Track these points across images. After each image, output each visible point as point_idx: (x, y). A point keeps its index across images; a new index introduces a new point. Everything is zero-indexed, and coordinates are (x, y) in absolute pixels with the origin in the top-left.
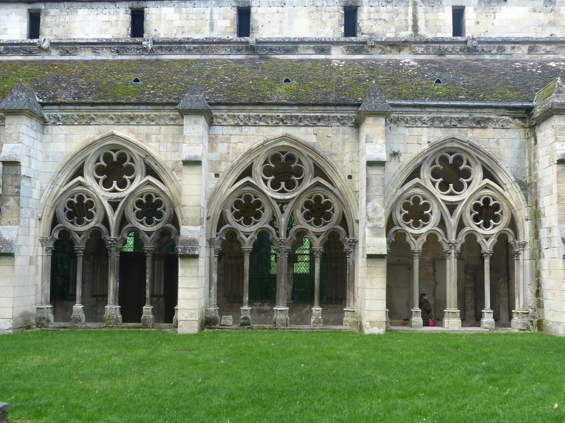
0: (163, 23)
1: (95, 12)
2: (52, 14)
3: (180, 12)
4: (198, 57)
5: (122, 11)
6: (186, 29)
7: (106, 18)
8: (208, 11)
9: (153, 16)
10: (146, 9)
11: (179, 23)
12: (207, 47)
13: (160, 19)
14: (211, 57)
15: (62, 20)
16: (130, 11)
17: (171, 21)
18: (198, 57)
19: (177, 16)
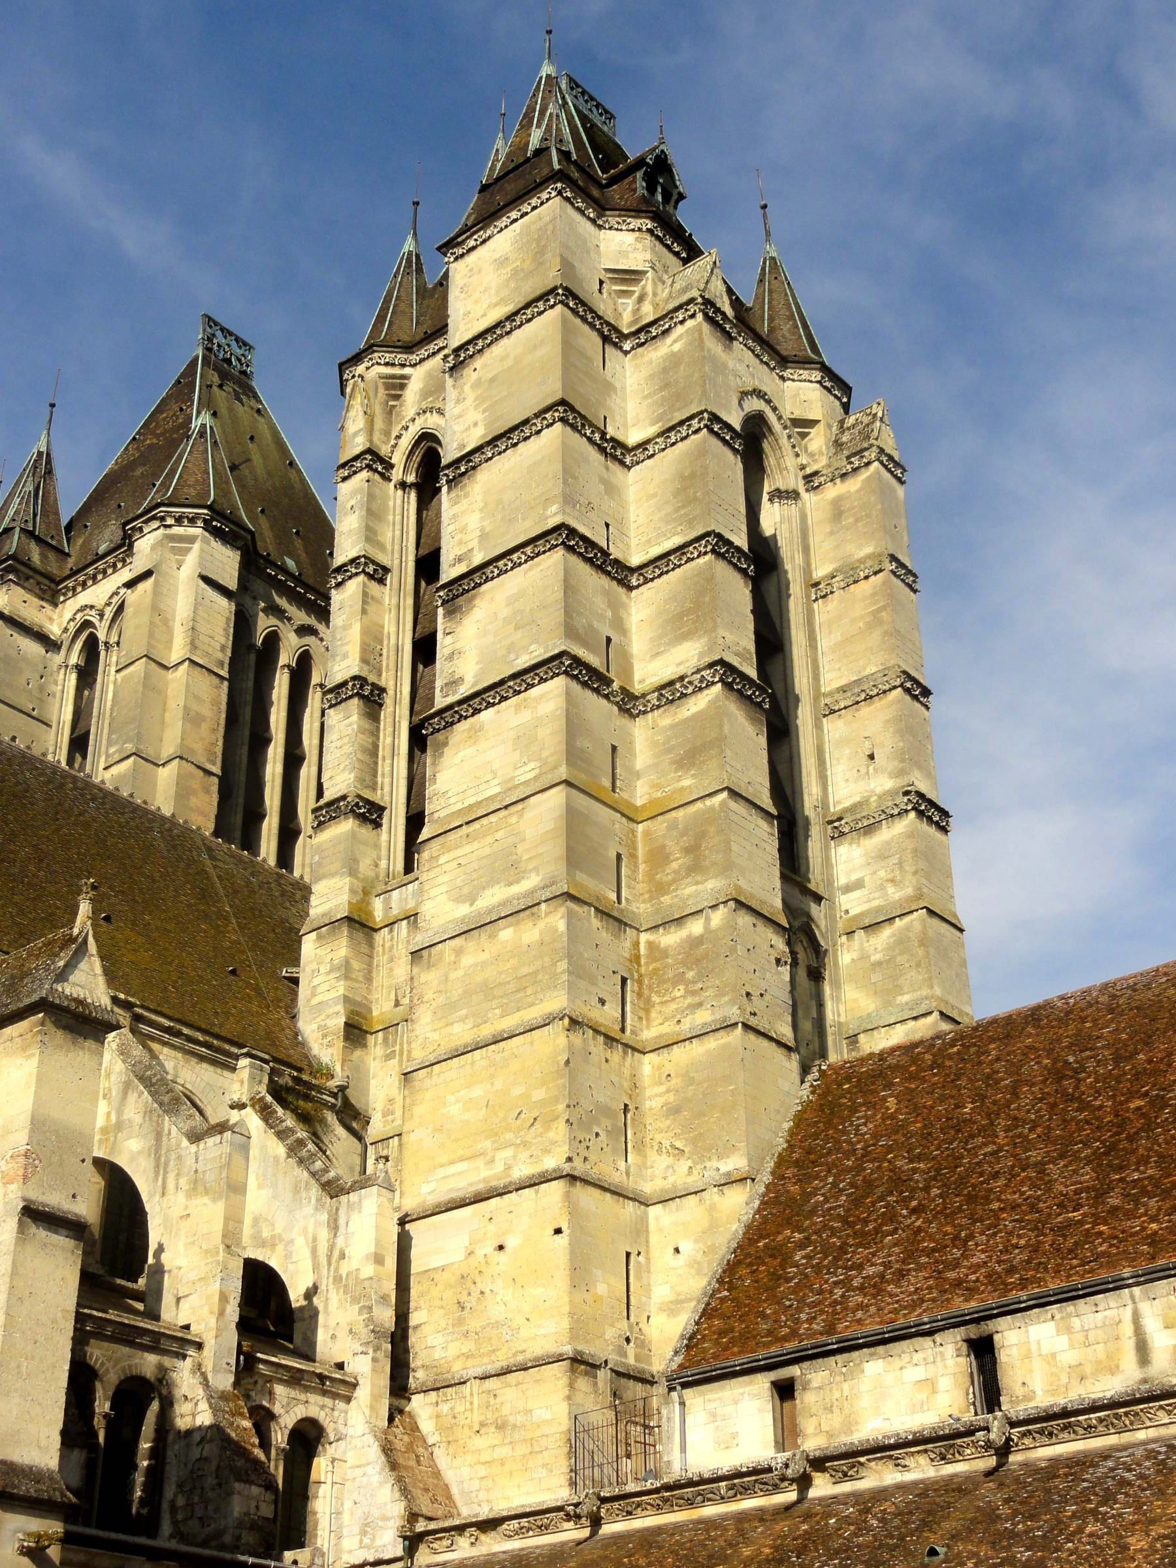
0: (1037, 1365)
1: (897, 1363)
2: (814, 1384)
3: (1069, 1330)
4: (1113, 1440)
5: (949, 1350)
6: (1088, 1369)
7: (920, 1373)
8: (1128, 1313)
9: (1014, 1351)
10: (996, 1337)
11: (1069, 1357)
12: (1126, 1414)
13: (1028, 1356)
14: (1141, 1435)
15: (837, 1394)
16: (964, 1347)
17: (1054, 1355)
18: (1113, 1440)
19: (1062, 1341)
